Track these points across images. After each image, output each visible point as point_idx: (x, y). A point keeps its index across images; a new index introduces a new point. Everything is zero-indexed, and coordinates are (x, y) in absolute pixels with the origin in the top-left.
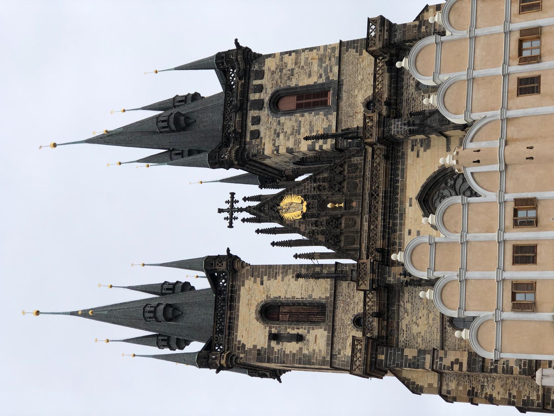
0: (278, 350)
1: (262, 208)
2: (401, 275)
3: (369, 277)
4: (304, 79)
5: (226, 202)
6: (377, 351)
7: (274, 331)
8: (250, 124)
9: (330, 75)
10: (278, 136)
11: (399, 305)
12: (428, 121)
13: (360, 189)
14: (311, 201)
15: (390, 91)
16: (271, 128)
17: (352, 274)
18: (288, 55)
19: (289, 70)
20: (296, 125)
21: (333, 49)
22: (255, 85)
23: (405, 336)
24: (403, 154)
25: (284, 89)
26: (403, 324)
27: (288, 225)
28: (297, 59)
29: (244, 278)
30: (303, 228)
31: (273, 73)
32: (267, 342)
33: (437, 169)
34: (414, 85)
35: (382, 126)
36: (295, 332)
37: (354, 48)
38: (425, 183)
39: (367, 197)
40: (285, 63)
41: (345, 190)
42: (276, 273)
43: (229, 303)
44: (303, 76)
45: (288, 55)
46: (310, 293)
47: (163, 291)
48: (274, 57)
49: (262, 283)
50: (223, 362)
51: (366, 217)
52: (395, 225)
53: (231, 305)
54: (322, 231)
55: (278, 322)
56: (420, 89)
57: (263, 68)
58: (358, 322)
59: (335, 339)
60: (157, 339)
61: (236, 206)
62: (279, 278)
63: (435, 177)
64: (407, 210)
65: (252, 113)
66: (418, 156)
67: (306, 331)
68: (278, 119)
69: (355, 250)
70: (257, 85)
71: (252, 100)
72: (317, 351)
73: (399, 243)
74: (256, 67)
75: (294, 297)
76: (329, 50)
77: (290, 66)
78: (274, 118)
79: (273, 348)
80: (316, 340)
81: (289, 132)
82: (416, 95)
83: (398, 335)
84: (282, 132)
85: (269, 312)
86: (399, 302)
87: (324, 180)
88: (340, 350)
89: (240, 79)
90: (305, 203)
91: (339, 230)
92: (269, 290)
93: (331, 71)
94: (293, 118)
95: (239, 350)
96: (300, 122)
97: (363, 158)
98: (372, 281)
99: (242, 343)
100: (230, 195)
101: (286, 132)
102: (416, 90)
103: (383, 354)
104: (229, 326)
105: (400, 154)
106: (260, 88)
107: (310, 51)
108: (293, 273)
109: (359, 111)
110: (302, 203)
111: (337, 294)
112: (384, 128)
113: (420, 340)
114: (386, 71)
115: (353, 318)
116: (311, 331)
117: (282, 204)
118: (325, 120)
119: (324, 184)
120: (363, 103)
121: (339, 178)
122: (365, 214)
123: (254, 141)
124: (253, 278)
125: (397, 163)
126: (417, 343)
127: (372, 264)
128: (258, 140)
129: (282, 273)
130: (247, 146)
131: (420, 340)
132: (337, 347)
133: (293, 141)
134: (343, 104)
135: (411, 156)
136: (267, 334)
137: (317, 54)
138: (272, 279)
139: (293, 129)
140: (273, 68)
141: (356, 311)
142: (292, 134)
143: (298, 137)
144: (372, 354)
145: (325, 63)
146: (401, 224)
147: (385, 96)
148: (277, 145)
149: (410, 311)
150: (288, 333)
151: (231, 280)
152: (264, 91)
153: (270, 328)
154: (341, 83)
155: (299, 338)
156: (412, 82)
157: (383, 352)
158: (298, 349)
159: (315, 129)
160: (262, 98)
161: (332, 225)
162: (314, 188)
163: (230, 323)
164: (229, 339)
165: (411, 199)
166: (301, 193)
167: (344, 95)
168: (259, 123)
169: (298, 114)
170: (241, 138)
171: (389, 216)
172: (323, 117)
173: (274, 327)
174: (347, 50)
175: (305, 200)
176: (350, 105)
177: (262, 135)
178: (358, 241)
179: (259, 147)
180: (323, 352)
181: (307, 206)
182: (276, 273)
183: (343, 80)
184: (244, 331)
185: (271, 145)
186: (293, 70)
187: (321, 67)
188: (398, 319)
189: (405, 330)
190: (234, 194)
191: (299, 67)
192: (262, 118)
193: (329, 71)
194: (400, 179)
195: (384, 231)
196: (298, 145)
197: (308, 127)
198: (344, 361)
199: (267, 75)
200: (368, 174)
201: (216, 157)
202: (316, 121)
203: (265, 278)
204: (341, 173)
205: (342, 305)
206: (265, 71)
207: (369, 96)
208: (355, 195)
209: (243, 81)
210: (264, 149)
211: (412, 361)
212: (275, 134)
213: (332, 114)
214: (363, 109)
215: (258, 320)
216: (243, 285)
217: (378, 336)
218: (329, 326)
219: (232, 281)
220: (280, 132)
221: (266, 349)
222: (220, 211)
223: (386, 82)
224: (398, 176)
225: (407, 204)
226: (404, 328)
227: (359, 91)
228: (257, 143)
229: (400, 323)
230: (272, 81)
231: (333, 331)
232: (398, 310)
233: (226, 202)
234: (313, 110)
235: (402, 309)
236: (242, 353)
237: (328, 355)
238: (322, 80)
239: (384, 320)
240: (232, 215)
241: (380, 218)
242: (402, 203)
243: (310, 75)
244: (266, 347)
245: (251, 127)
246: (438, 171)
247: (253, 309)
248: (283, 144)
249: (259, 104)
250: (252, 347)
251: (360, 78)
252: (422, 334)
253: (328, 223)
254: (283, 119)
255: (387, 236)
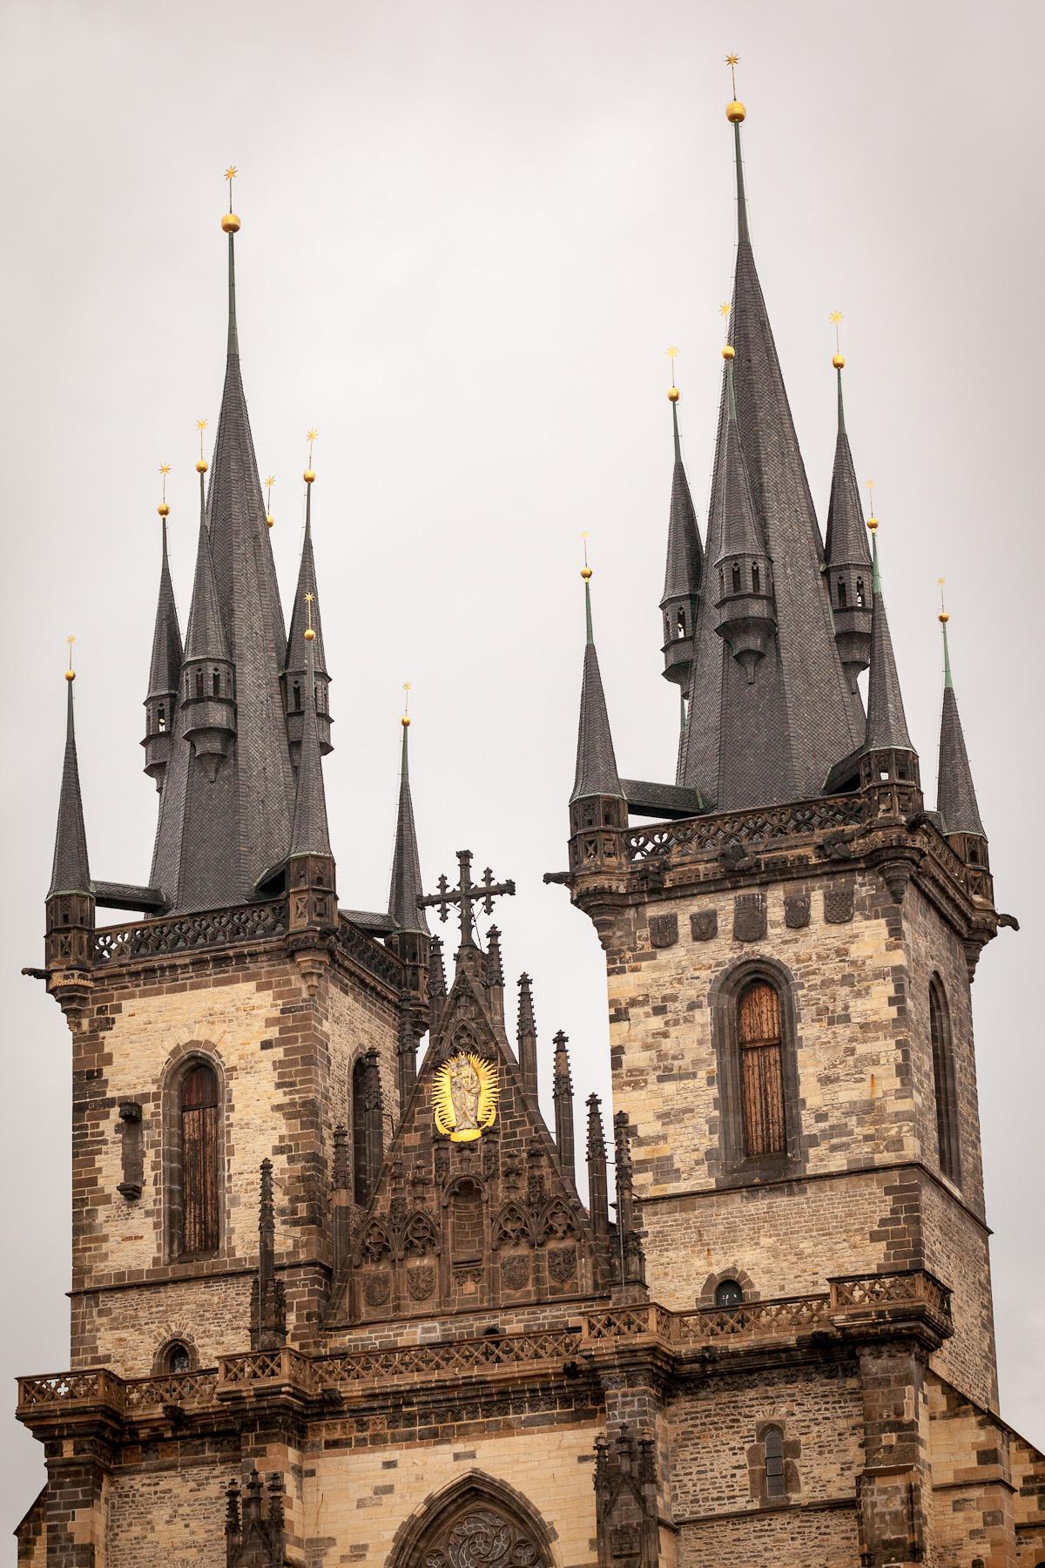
0: (102, 1133)
1: (463, 1000)
2: (255, 1473)
3: (246, 1388)
4: (818, 1062)
5: (488, 871)
6: (80, 1435)
7: (148, 1108)
8: (694, 909)
9: (822, 1150)
10: (659, 1010)
11: (214, 1462)
12: (626, 1497)
13: (509, 1297)
14: (481, 1150)
15: (749, 1353)
16: (680, 981)
17: (267, 1328)
18: (892, 993)
19: (846, 1008)
20: (685, 1063)
21: (897, 1144)
22: (806, 900)
23: (145, 1489)
24: (590, 1415)
25: (790, 999)
26: (171, 1482)
27: (419, 1090)
28: (878, 1026)
29: (278, 985)
30: (412, 1139)
31: (842, 953)
32: (121, 1094)
33: (546, 1518)
34: (776, 1417)
35: (624, 1361)
36: (149, 1174)
37: (893, 1211)
38: (513, 1491)
39: (488, 1322)
40: (867, 989)
41: (508, 1252)
42: (292, 1084)
43: (208, 956)
44: (824, 1057)
45: (892, 993)
46: (244, 1198)
47: (290, 679)
48: (889, 948)
49: (266, 1045)
50: (58, 980)
51: (434, 1331)
52: (410, 1420)
53: (206, 962)
54: (404, 1205)
55: (176, 1112)
56: (761, 1437)
57: (857, 916)
58: (176, 1351)
59: (133, 1295)
60: (164, 696)
61: (478, 906)
62: (280, 1098)
63: (529, 1516)
64: (445, 1447)
65: (725, 906)
66: (583, 1459)
67: (150, 1206)
68: (705, 1001)
69: (354, 1312)
70: (807, 908)
71: (764, 900)
72: (105, 1247)
73: (365, 1439)
74: (864, 887)
75: (231, 1152)
76: (893, 1132)
77: (858, 1008)
78: (708, 986)
79: (107, 1116)
80: (130, 1238)
81: (667, 1045)
82: (747, 1426)
83: (147, 1471)
84: (667, 1023)
85: (197, 1077)
86: (223, 1462)
87: (535, 1182)
88: (109, 1312)
89: (820, 847)
90: (472, 1135)
91: (401, 1254)
92: (248, 1070)
93: (834, 1148)
94: (706, 1051)
95: (100, 1011)
96: (694, 1075)
97: (590, 1291)
98: (236, 1398)
99: (116, 1016)
100: (503, 882)
101: (665, 1035)
102: (759, 1424)
103: (77, 1452)
104: (153, 970)
105: (591, 1407)
106: (797, 919)
107: (898, 1067)
108: (292, 1137)
109: (714, 1258)
110: (479, 1124)
111: (242, 1279)
112: (621, 1366)
113: (136, 1530)
114: (802, 1333)
115: (184, 1337)
116: (150, 1220)
117: (474, 1059)
118: (695, 1156)
119: (523, 1184)
120: (734, 1269)
121: (535, 1230)
122: (443, 1324)
123: (646, 932)
124: (276, 1013)
125: (566, 1402)
126: (130, 1525)
127: (276, 1391)
128: (648, 949)
129: (293, 1104)
130: (631, 914)
131: (136, 1530)
132: (115, 1303)
133: (642, 1064)
134: (739, 1207)
135: (584, 1438)
136: (139, 1090)
137: (885, 1094)
138: (276, 1074)
139: (675, 1058)
140: (856, 951)
141: (201, 1342)
142: (662, 1056)
143: (652, 1078)
144: (68, 1426)
145: (861, 1123)
146: (410, 1437)
147: (734, 1344)
148: (632, 1011)
149: (202, 1494)
150: (144, 1155)
151: (268, 946)
152: (790, 935)
153: (156, 1096)
154: (796, 1189)
155: (131, 1193)
156: (784, 1410)
157: (83, 1451)
158: (107, 1191)
159: (671, 1129)
160: (770, 931)
161: (414, 1229)
162: (511, 1156)
163: (162, 969)
164: (121, 975)
165: (472, 1455)
166: (505, 1116)
167: (758, 1206)
168: (696, 939)
169: (715, 1066)
170: (652, 892)
171: (426, 1403)
172: (703, 1148)
173: (157, 1106)
174: (888, 1191)
175: (484, 1134)
176: (731, 1228)
177: (663, 956)
178: (377, 1314)
179: (629, 955)
180: (102, 1265)
181: (461, 1147)
182: (292, 1084)
183: (804, 1191)
184: (144, 1018)
185: (633, 994)
186: (846, 1019)
187: (847, 1114)
188: (183, 1466)
189: (158, 1488)
190: (512, 893)
191: (852, 1040)
192: (712, 946)
193: (835, 1141)
194: (523, 1416)
195: (386, 1395)
196: (628, 1083)
197: (679, 1104)
198: (83, 1331)
199: (835, 935)
200: (547, 1316)
201: (590, 823)
202: (694, 1127)
203: (278, 1053)
204: (551, 1231)
205: (216, 1299)
206: (848, 927)
207: (751, 1284)
208: (493, 1288)
209: (813, 861)
210: (622, 971)
211: (62, 1534)
212: (664, 999)
213: (710, 1175)
214: (716, 1270)
215: (173, 1053)
216: (259, 988)
217: (133, 1423)
218: (165, 1271)
219: (266, 952)
220: (670, 1016)
221: (104, 1093)
222: (464, 857)
223: (773, 1337)
224: (533, 1407)
225: (459, 1447)
226: (163, 1485)
227: (769, 1249)
228: (640, 943)
229: (173, 1473)
230: (819, 957)
231: (152, 1284)
232: (203, 1463)
233: (488, 871)
234: (725, 1112)
235: (205, 1472)
236: (91, 1022)
237: (99, 1279)
238: (809, 1125)
239: (174, 1429)
240: (454, 898)
241: (416, 1377)
242: (464, 1433)
243: (826, 1080)
244: (109, 1095)
245: (685, 913)
246: (541, 1520)
247: (201, 1033)
248: (632, 1033)
249: (751, 927)
250: (106, 1050)
251: (806, 1246)
252: (151, 1537)
253: (418, 1218)
254: (704, 1016)
255: (375, 1405)
